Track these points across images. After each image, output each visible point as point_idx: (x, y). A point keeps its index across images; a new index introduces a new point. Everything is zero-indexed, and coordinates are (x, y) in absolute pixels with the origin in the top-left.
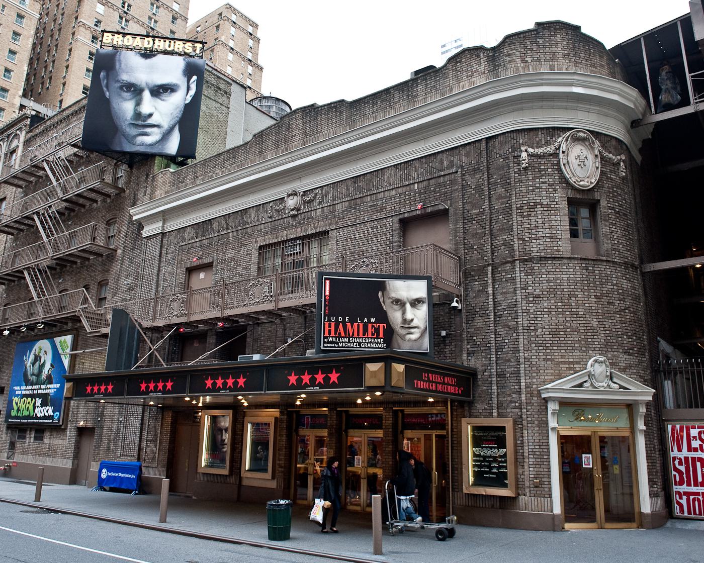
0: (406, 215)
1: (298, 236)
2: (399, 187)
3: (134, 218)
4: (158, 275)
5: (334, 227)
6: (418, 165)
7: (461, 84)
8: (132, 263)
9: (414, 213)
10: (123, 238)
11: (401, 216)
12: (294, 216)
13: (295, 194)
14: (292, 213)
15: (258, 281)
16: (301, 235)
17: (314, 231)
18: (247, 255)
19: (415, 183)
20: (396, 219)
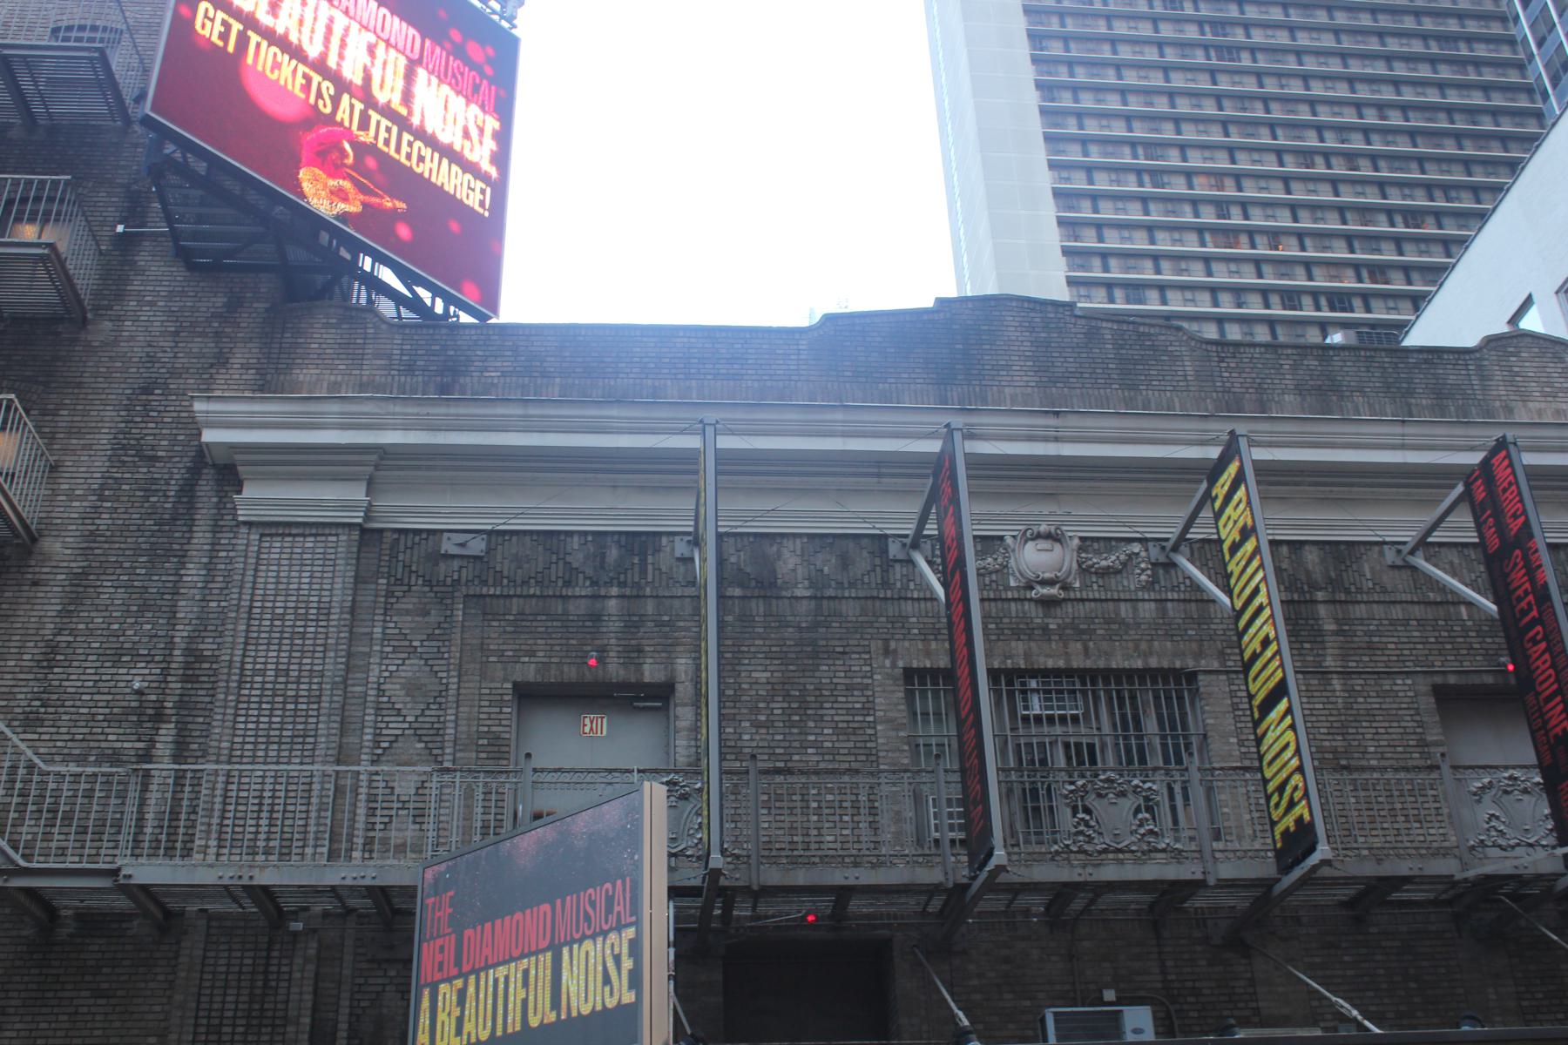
0: (1452, 680)
1: (1075, 665)
2: (1412, 602)
3: (209, 436)
4: (345, 681)
5: (1215, 665)
6: (1456, 561)
7: (1531, 405)
8: (145, 607)
9: (1476, 680)
10: (71, 496)
11: (1439, 680)
12: (1048, 603)
13: (1054, 537)
14: (1045, 591)
15: (1108, 780)
16: (1089, 664)
17: (1139, 664)
18: (850, 688)
19: (1459, 603)
20: (1423, 685)
